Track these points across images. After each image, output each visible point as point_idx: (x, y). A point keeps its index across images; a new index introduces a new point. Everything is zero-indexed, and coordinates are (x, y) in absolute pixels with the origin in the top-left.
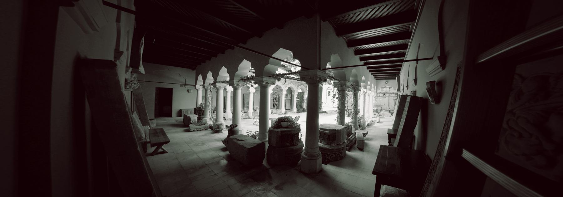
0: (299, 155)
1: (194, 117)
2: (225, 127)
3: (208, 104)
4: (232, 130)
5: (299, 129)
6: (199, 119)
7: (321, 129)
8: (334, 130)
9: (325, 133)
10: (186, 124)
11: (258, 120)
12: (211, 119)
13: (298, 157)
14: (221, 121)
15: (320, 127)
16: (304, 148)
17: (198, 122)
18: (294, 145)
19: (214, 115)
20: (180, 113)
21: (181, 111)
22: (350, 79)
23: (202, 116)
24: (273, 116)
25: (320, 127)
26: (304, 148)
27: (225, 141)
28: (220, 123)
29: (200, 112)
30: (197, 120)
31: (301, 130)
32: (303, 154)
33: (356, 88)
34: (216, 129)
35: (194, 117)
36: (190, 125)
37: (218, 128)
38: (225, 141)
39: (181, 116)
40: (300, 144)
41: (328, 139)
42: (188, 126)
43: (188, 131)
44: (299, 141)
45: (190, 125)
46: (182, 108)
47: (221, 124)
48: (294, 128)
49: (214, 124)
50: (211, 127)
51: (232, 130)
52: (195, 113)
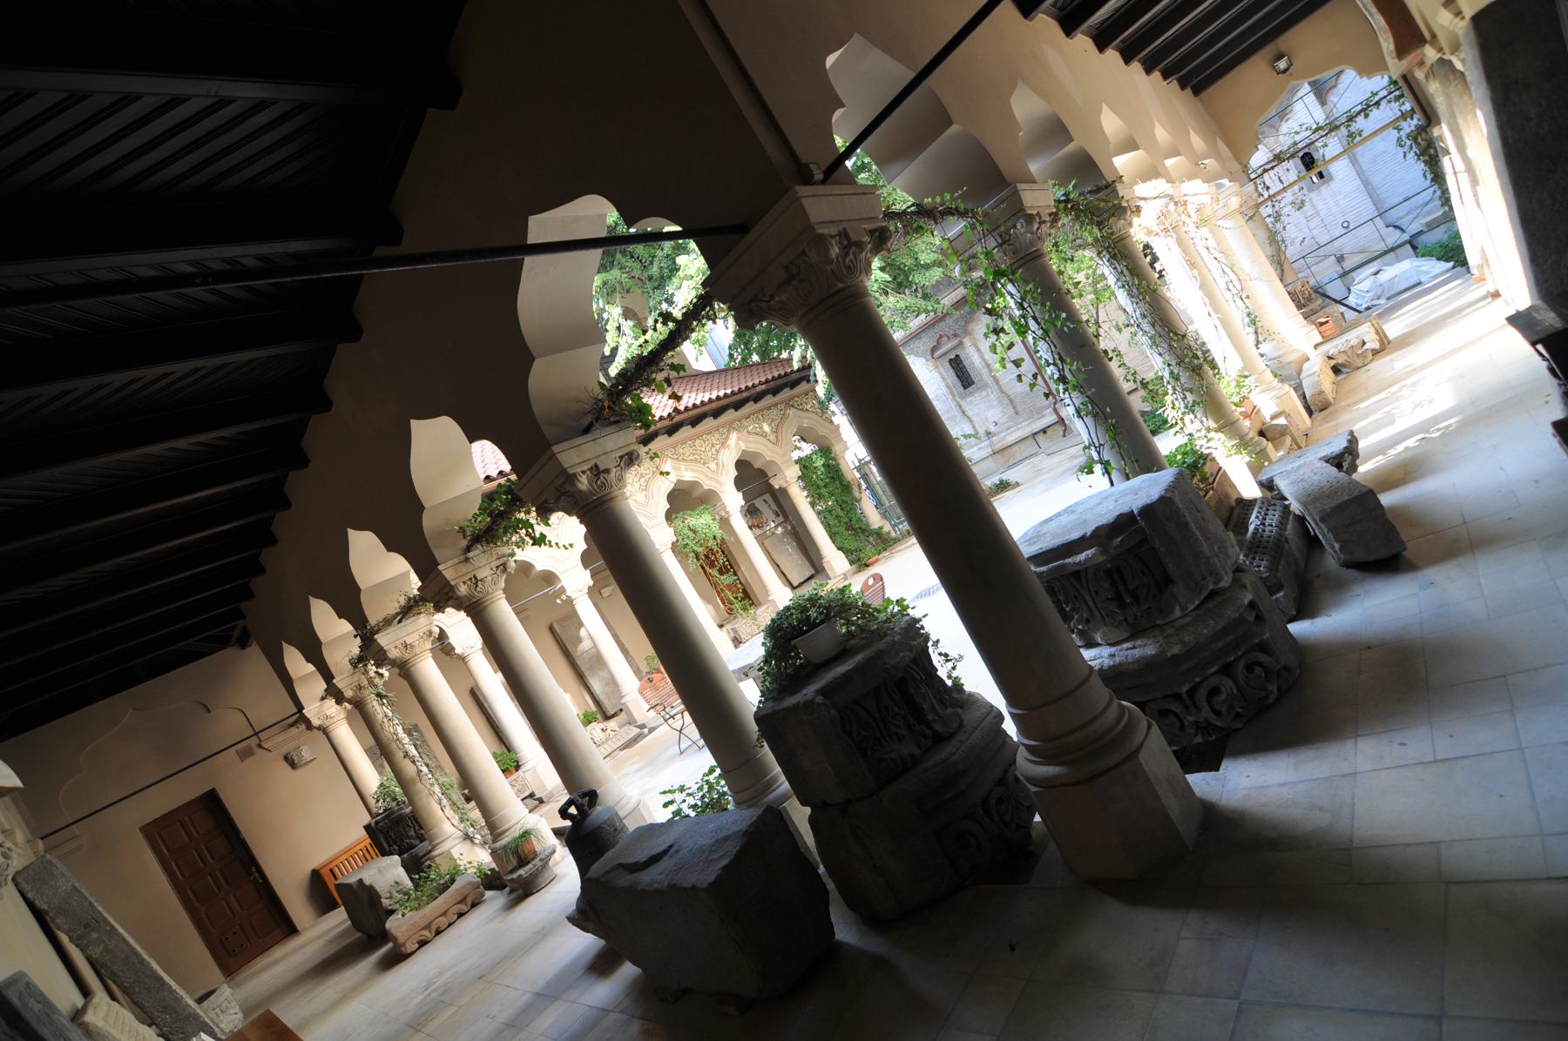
0: (1007, 779)
1: (388, 873)
2: (553, 841)
3: (409, 769)
4: (587, 832)
5: (913, 637)
6: (415, 866)
7: (1041, 558)
8: (1124, 523)
9: (1077, 574)
10: (371, 935)
11: (688, 718)
12: (468, 837)
13: (1008, 794)
14: (517, 816)
15: (1027, 550)
16: (1010, 727)
17: (417, 886)
18: (940, 739)
19: (476, 814)
20: (322, 891)
21: (316, 875)
22: (1034, 167)
23: (422, 848)
24: (737, 652)
25: (1027, 550)
26: (1010, 727)
27: (585, 915)
28: (515, 833)
29: (398, 831)
30: (408, 884)
31: (930, 626)
32: (1025, 764)
33: (1098, 203)
34: (514, 875)
35: (388, 873)
36: (391, 924)
37: (523, 862)
38: (585, 915)
39: (332, 906)
40: (970, 717)
41: (1118, 598)
42: (385, 936)
43: (397, 958)
44: (955, 696)
45: (391, 924)
46: (316, 861)
47: (526, 835)
48: (880, 634)
49: (494, 853)
50: (491, 881)
51: (587, 832)
52: (384, 853)
